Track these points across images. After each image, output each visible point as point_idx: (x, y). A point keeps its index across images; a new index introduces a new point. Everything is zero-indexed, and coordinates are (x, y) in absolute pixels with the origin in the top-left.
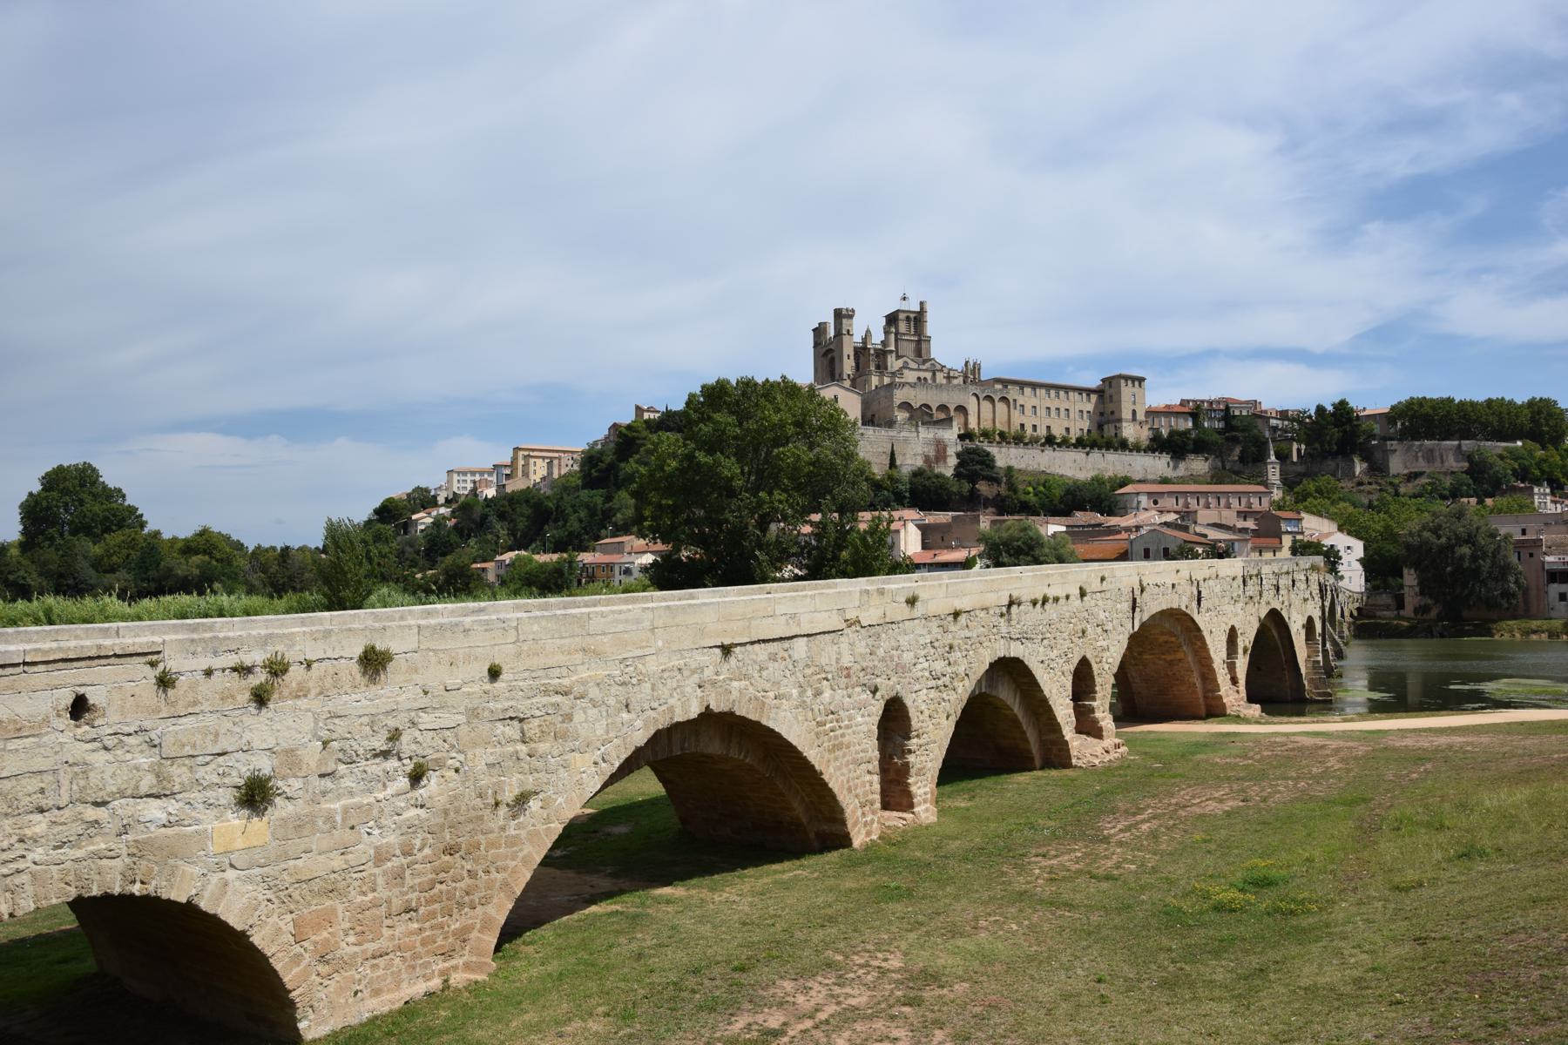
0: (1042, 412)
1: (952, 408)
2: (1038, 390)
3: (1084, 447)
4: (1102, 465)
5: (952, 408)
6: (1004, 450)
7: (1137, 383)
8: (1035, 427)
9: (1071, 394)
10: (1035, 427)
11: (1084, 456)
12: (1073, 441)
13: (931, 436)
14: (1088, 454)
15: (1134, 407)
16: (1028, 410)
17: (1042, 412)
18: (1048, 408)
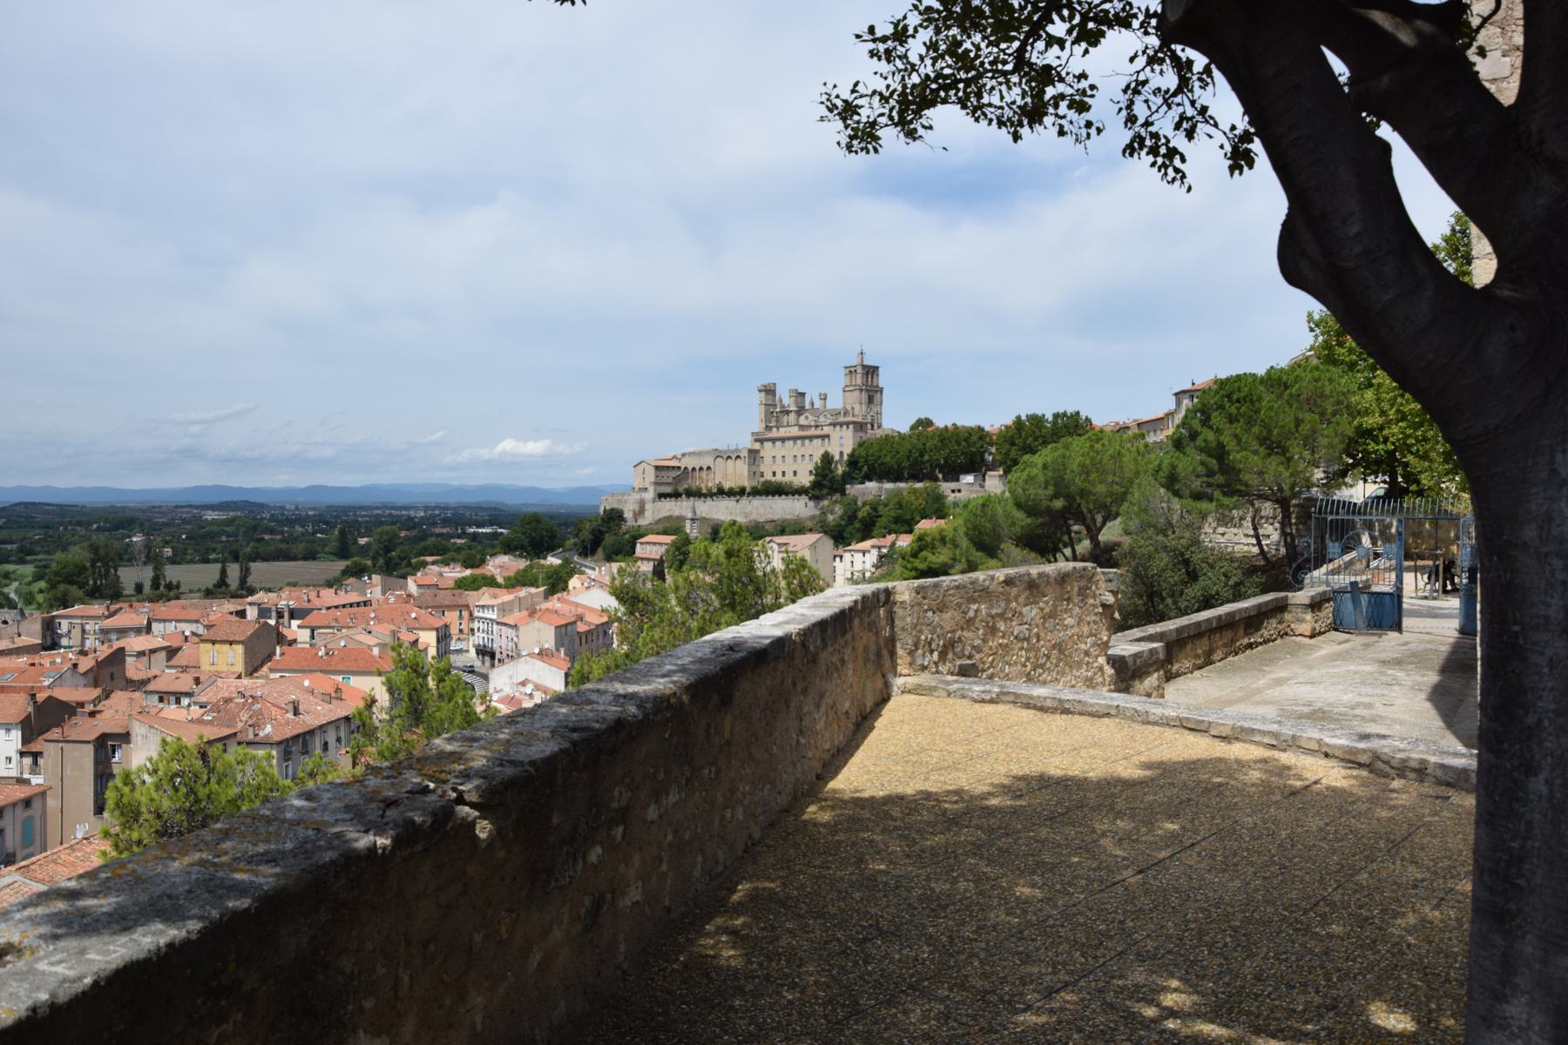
0: (789, 460)
1: (705, 468)
2: (787, 442)
3: (734, 496)
4: (749, 508)
5: (705, 468)
6: (679, 503)
7: (845, 427)
8: (784, 473)
9: (815, 441)
10: (784, 473)
11: (735, 503)
12: (715, 490)
13: (638, 497)
14: (738, 501)
15: (840, 449)
16: (779, 459)
17: (789, 460)
18: (795, 456)
